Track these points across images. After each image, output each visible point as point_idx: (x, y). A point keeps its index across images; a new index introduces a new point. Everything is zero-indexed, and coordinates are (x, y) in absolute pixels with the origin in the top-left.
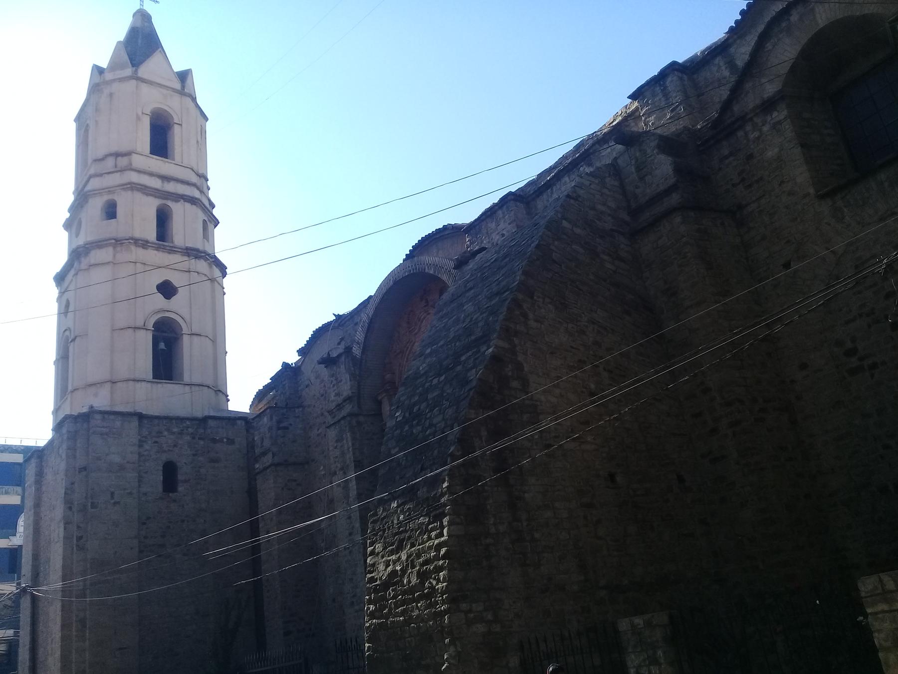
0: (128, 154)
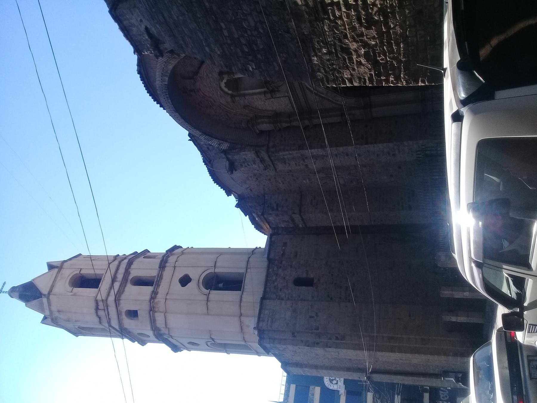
0: (97, 302)
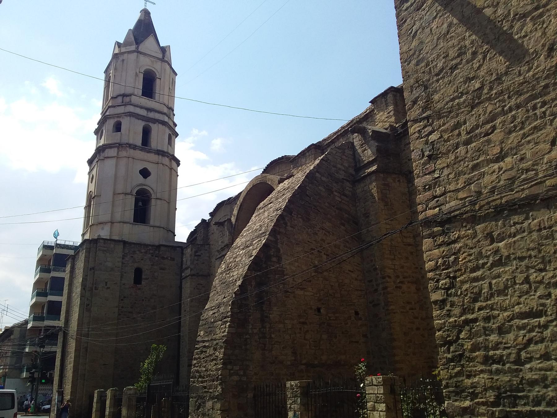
0: (130, 95)
